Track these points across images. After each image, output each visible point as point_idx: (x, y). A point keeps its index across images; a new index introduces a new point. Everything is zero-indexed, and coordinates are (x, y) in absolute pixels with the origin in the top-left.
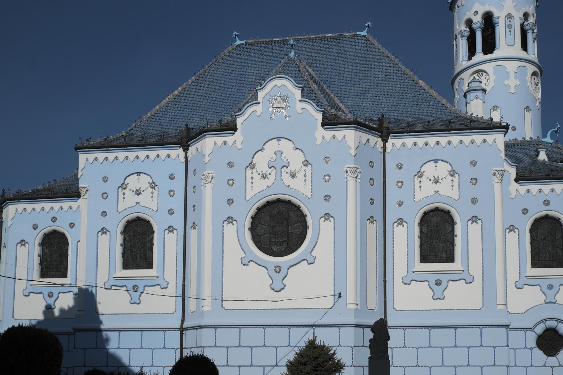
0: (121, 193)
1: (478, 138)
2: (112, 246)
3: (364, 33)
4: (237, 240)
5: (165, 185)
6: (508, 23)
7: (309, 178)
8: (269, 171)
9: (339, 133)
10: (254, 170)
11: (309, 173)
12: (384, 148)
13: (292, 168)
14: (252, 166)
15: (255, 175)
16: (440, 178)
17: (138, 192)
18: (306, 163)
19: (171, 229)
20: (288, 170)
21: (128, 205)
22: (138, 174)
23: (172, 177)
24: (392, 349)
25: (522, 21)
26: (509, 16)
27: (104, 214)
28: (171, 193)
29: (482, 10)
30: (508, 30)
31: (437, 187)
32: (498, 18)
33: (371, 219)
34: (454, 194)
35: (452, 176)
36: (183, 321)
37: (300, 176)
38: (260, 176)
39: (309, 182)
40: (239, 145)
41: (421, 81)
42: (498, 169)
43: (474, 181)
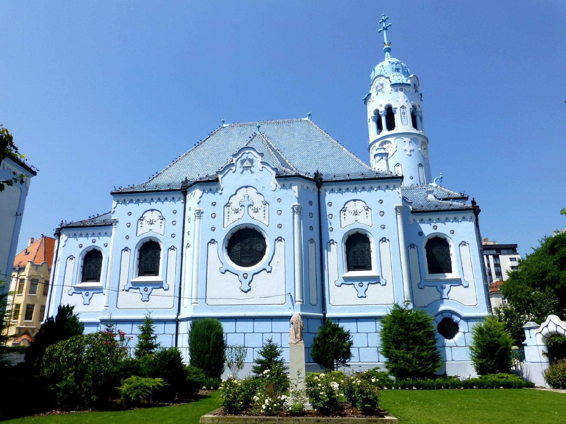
0: (139, 223)
2: (130, 260)
3: (307, 119)
4: (219, 256)
5: (170, 217)
6: (402, 111)
8: (240, 208)
10: (230, 208)
12: (319, 192)
15: (231, 211)
16: (358, 212)
17: (151, 223)
18: (265, 203)
19: (172, 248)
20: (253, 208)
21: (146, 231)
25: (412, 110)
26: (403, 107)
27: (127, 237)
28: (174, 223)
29: (385, 103)
30: (402, 115)
31: (356, 218)
32: (396, 108)
33: (311, 241)
34: (368, 222)
35: (367, 210)
36: (179, 314)
37: (261, 211)
38: (234, 212)
39: (267, 216)
42: (398, 205)
43: (382, 213)
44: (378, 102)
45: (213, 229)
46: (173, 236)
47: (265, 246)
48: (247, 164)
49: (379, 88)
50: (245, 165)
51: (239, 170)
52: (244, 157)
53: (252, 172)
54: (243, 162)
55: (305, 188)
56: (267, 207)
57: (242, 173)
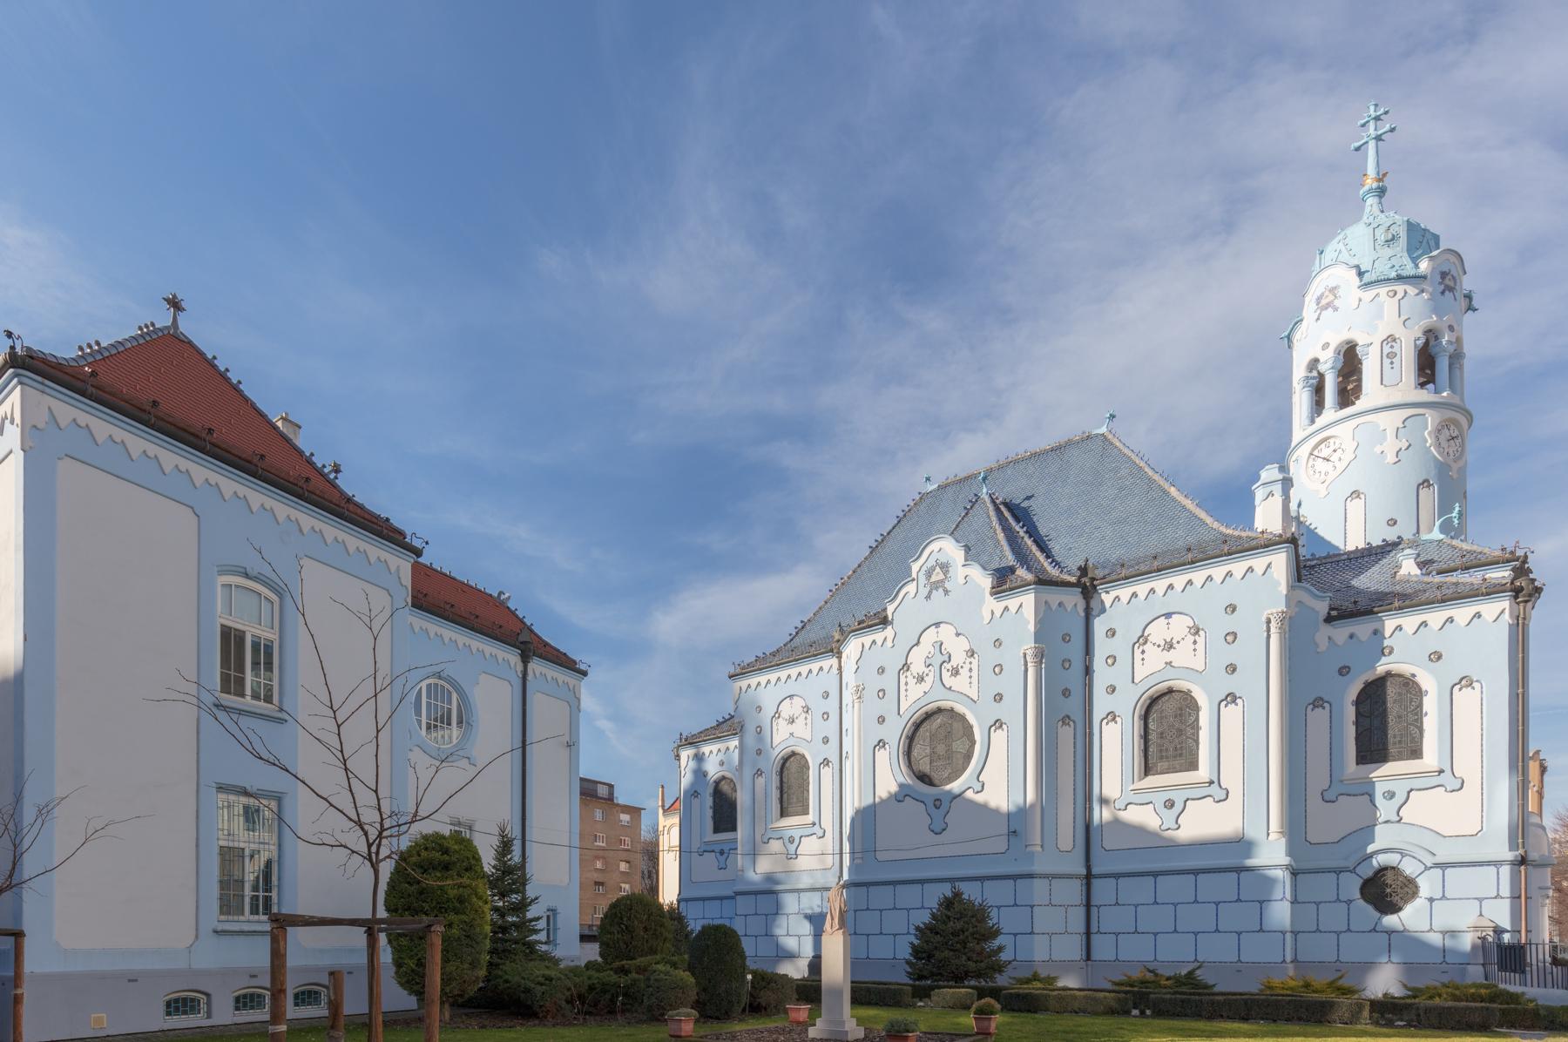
1: (1238, 567)
5: (819, 706)
7: (975, 674)
9: (1013, 603)
11: (975, 667)
13: (954, 663)
14: (906, 666)
17: (792, 721)
18: (971, 653)
20: (949, 666)
22: (791, 697)
23: (826, 695)
24: (1098, 907)
29: (1336, 339)
33: (1066, 720)
37: (964, 672)
39: (975, 680)
40: (889, 643)
41: (1173, 490)
44: (1315, 343)
45: (881, 720)
46: (826, 740)
47: (973, 743)
48: (938, 575)
49: (1324, 302)
50: (934, 578)
51: (924, 591)
52: (931, 562)
53: (946, 592)
54: (929, 574)
55: (1054, 606)
56: (975, 662)
57: (928, 597)
